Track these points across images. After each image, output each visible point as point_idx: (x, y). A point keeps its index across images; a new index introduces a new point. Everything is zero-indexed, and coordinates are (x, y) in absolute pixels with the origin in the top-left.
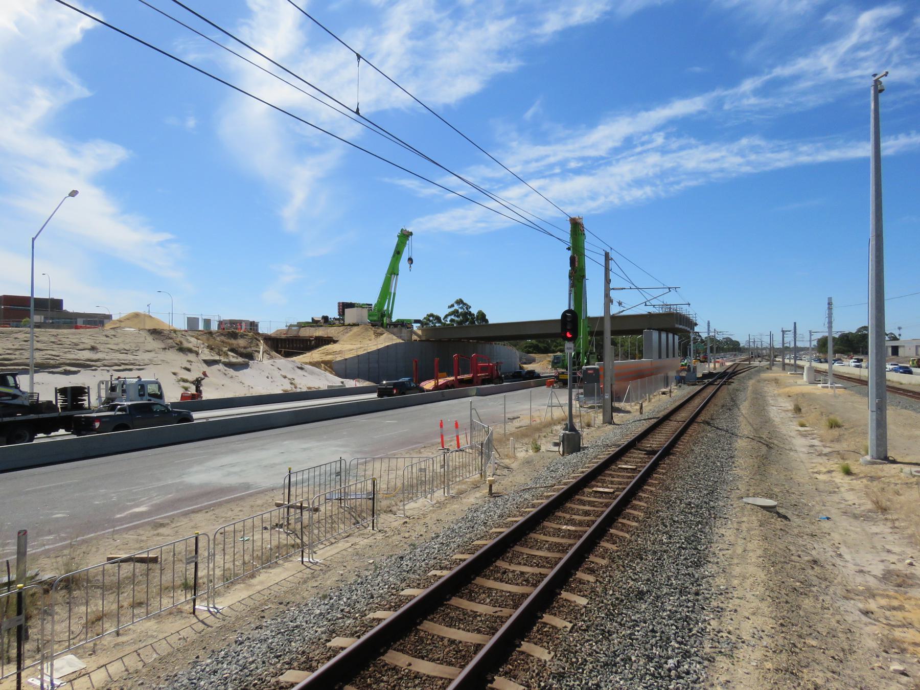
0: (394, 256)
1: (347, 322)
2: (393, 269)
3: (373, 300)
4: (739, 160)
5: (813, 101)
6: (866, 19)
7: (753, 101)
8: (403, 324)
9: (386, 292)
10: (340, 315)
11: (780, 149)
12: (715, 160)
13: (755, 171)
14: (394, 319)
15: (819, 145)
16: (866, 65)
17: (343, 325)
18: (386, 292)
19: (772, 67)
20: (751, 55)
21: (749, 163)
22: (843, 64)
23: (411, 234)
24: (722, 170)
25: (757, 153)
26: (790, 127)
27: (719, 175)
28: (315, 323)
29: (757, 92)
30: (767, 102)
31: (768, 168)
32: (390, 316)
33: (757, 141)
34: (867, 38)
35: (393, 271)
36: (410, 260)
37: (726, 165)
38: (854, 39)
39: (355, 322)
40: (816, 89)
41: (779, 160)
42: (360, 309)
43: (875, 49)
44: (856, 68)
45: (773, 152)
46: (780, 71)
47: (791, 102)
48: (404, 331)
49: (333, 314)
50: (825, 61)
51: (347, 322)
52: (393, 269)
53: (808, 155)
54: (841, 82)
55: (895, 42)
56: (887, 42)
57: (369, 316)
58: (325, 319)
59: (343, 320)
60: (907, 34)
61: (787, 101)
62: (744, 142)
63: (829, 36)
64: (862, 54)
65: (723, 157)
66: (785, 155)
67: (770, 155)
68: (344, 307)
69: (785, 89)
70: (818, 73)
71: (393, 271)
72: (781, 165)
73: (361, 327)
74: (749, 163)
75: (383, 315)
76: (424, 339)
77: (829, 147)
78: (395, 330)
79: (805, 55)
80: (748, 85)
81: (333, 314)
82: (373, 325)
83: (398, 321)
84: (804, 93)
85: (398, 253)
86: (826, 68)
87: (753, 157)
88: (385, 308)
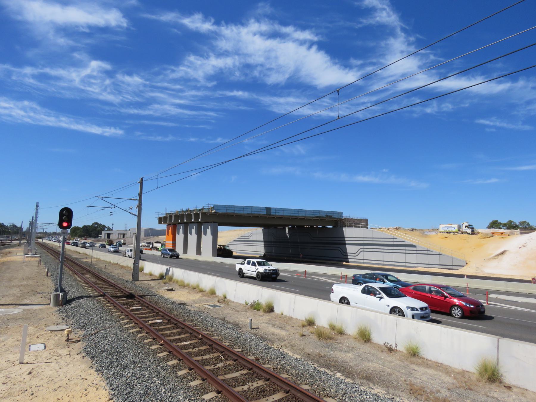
4: (22, 113)
5: (68, 95)
6: (95, 64)
7: (32, 81)
11: (49, 115)
12: (5, 108)
13: (33, 123)
15: (72, 119)
16: (95, 87)
19: (44, 66)
20: (30, 54)
21: (30, 117)
22: (83, 81)
24: (10, 116)
25: (34, 112)
26: (55, 104)
27: (9, 118)
29: (34, 76)
30: (42, 85)
31: (41, 124)
33: (34, 105)
34: (95, 74)
37: (13, 114)
38: (87, 72)
40: (69, 89)
41: (50, 121)
43: (99, 81)
44: (89, 87)
45: (45, 115)
46: (48, 70)
47: (55, 90)
50: (74, 76)
53: (66, 123)
54: (83, 91)
55: (108, 82)
56: (104, 80)
60: (113, 80)
61: (53, 89)
62: (26, 103)
63: (77, 64)
64: (93, 81)
65: (12, 108)
66: (52, 119)
67: (43, 116)
69: (52, 82)
70: (72, 81)
72: (51, 124)
74: (30, 117)
77: (78, 123)
79: (63, 68)
80: (28, 70)
84: (63, 88)
86: (75, 80)
87: (32, 114)
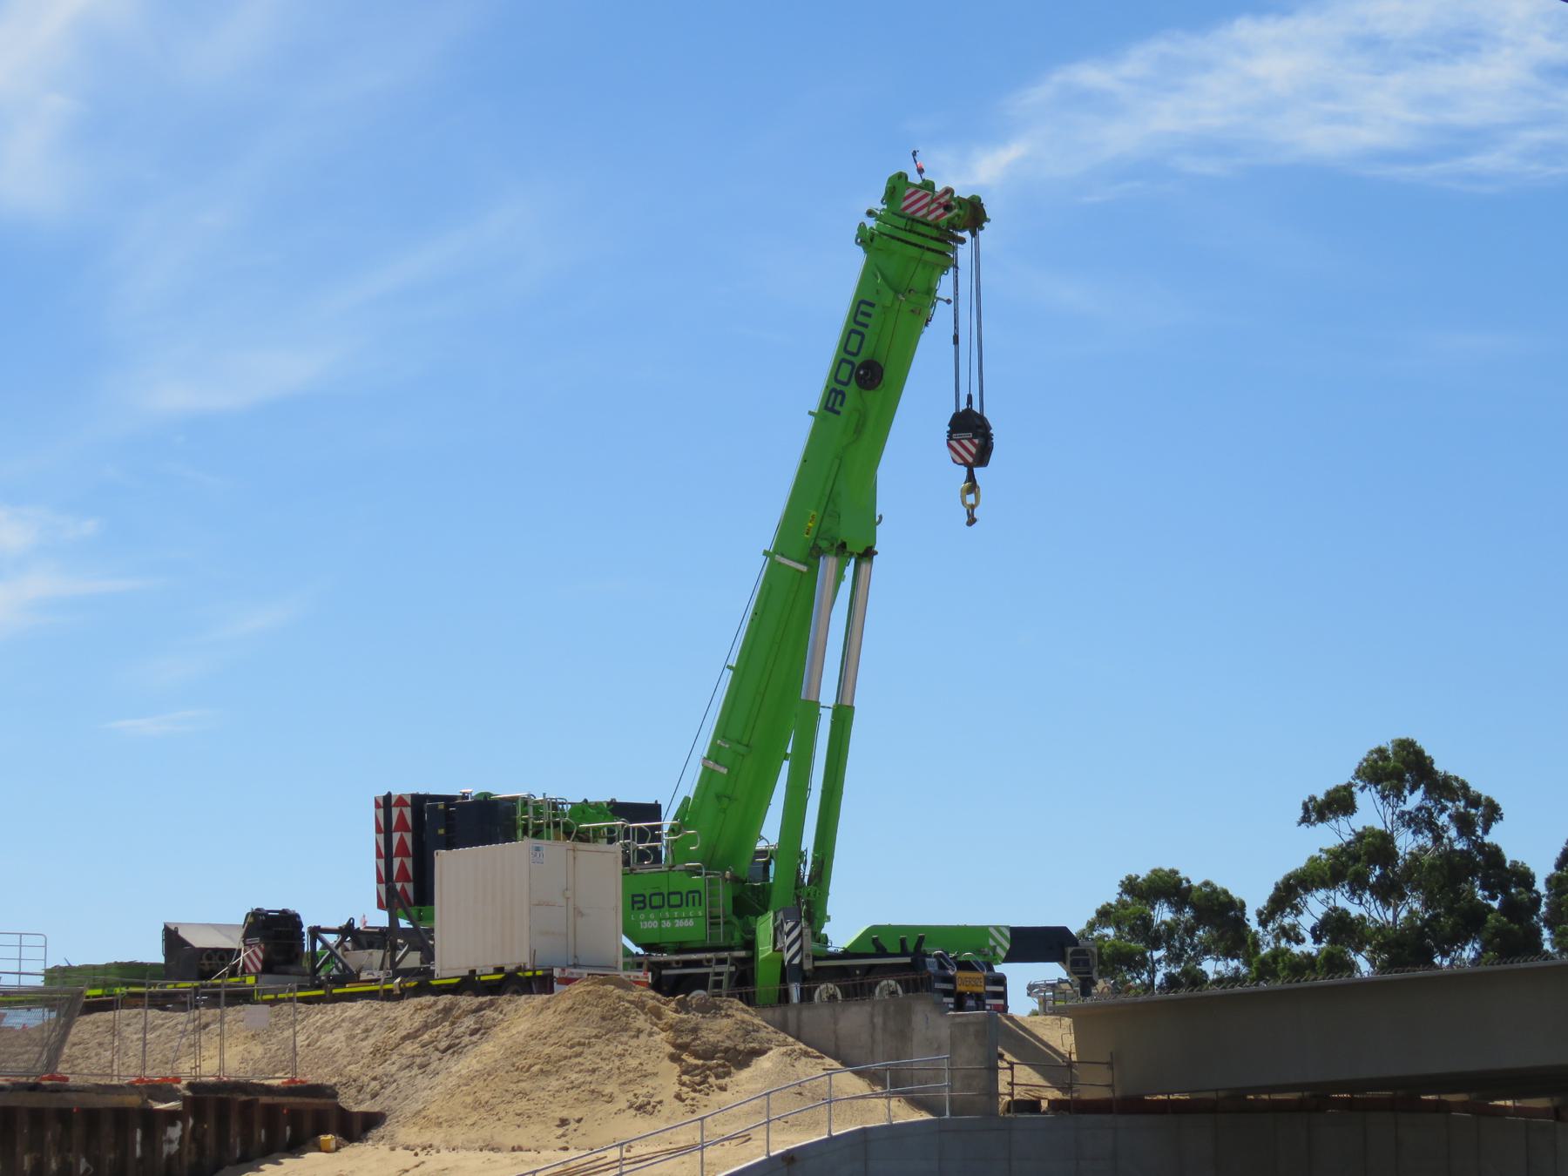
0: (833, 400)
1: (450, 961)
2: (830, 506)
3: (663, 767)
8: (926, 970)
9: (776, 706)
10: (390, 901)
14: (841, 932)
17: (423, 984)
18: (776, 706)
23: (973, 214)
28: (189, 973)
32: (809, 905)
35: (827, 531)
36: (971, 433)
39: (516, 956)
42: (555, 850)
48: (932, 1025)
49: (339, 890)
51: (450, 961)
52: (830, 506)
57: (637, 902)
58: (276, 933)
59: (422, 941)
68: (424, 832)
71: (827, 531)
73: (565, 996)
75: (749, 900)
76: (1094, 1087)
78: (855, 1019)
81: (339, 890)
82: (668, 985)
83: (876, 941)
85: (865, 376)
88: (770, 833)
